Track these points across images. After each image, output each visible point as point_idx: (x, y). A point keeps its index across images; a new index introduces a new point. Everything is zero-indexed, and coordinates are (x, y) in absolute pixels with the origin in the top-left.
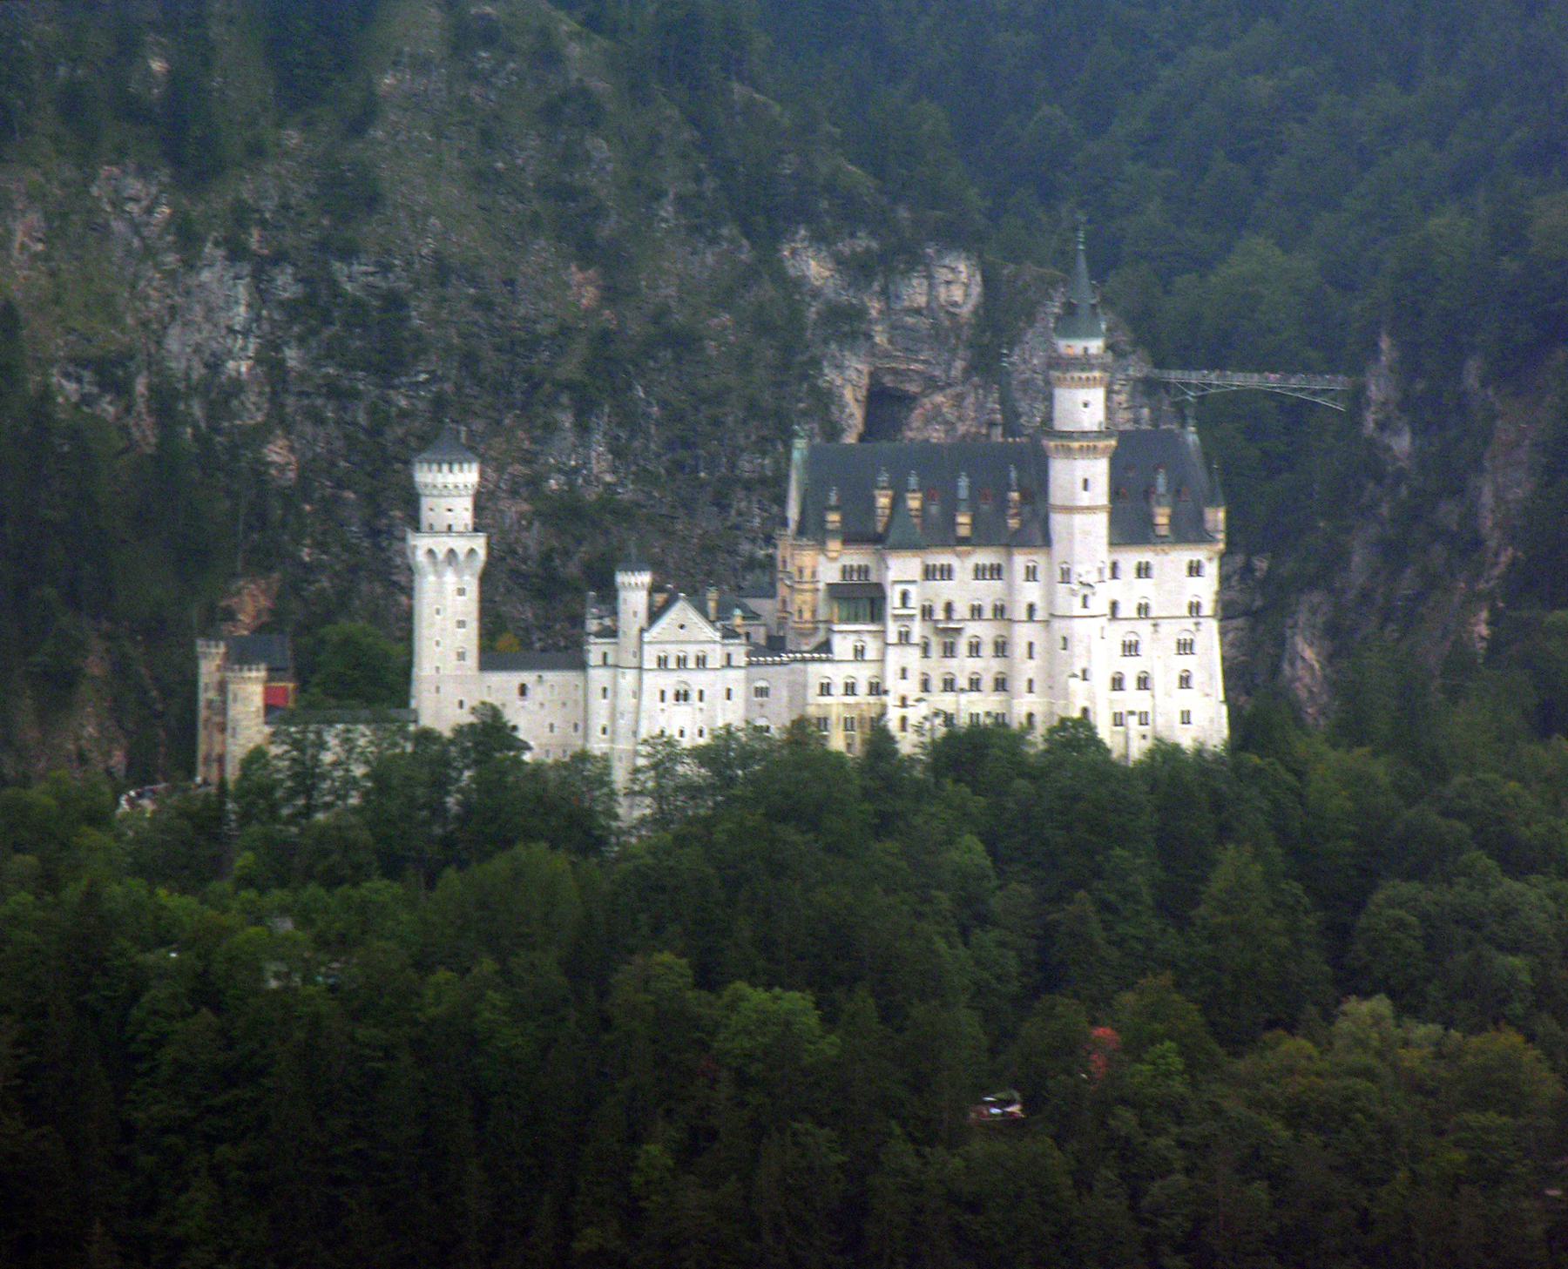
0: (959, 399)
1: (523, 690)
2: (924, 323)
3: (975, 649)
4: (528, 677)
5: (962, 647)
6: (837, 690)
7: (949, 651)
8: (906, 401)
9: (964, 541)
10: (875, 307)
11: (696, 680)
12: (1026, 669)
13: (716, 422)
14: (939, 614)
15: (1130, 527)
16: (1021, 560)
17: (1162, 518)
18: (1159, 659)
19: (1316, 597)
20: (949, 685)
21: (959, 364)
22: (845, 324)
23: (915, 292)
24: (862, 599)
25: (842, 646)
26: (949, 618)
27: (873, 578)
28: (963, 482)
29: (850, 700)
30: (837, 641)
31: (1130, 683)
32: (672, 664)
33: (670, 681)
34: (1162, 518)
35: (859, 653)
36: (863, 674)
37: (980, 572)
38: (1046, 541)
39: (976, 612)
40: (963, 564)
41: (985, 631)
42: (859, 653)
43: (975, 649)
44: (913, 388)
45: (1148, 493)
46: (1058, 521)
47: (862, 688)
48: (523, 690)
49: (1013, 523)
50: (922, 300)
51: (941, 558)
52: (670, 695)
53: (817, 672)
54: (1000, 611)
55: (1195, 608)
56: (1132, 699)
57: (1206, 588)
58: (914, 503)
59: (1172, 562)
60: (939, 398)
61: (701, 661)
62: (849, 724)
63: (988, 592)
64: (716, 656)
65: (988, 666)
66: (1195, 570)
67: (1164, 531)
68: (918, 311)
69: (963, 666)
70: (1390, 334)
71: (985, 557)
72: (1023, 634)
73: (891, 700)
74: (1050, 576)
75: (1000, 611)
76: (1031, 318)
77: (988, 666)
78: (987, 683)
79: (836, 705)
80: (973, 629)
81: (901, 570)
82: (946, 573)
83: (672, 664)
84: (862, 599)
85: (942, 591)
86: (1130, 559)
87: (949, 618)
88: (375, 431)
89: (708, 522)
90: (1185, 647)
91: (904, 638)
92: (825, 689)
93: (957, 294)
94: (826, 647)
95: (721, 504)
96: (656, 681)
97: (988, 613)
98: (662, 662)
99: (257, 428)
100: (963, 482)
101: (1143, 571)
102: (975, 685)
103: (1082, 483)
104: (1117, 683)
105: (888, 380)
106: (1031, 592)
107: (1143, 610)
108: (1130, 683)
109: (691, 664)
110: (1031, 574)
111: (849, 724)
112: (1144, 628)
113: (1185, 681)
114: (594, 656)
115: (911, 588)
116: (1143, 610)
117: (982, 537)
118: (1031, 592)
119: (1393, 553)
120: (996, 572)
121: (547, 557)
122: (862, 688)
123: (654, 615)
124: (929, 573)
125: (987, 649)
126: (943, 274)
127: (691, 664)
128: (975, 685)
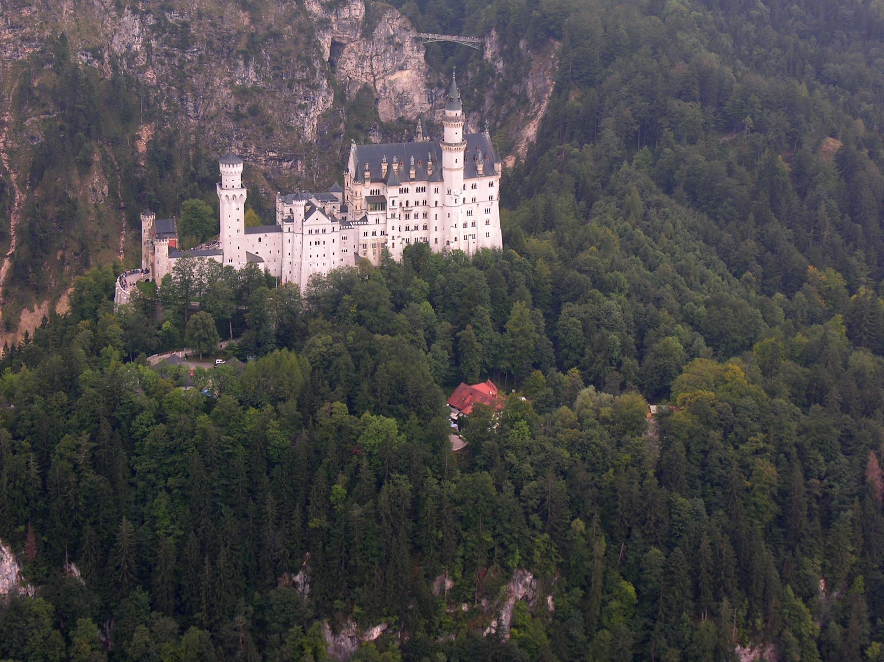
0: (359, 44)
1: (260, 240)
2: (349, 22)
3: (416, 216)
4: (262, 235)
5: (412, 216)
6: (370, 234)
7: (407, 217)
8: (342, 46)
9: (413, 180)
10: (333, 19)
11: (321, 237)
12: (434, 223)
13: (288, 61)
14: (404, 205)
15: (470, 172)
16: (433, 186)
17: (480, 168)
18: (479, 216)
19: (475, 114)
20: (407, 229)
21: (359, 34)
22: (324, 24)
23: (345, 13)
24: (378, 202)
25: (371, 219)
26: (407, 205)
27: (381, 194)
28: (412, 159)
29: (374, 237)
30: (369, 218)
31: (469, 225)
32: (314, 232)
33: (314, 238)
34: (480, 168)
35: (377, 221)
36: (379, 229)
37: (418, 190)
38: (442, 180)
39: (417, 203)
40: (412, 187)
41: (420, 210)
42: (377, 221)
43: (416, 216)
44: (344, 42)
45: (475, 158)
46: (445, 173)
47: (378, 233)
48: (260, 240)
49: (430, 173)
50: (347, 16)
51: (404, 186)
52: (313, 243)
53: (363, 229)
54: (425, 203)
55: (491, 198)
56: (470, 230)
57: (495, 191)
58: (395, 167)
59: (482, 182)
60: (352, 45)
61: (324, 231)
62: (374, 246)
63: (421, 197)
64: (329, 229)
65: (421, 222)
66: (491, 185)
67: (481, 173)
68: (346, 19)
69: (412, 222)
70: (496, 30)
71: (420, 184)
72: (433, 211)
73: (389, 238)
74: (443, 191)
75: (425, 203)
76: (380, 20)
77: (421, 222)
78: (421, 227)
79: (370, 239)
80: (416, 209)
81: (391, 193)
82: (407, 191)
83: (314, 232)
84: (378, 202)
85: (405, 197)
86: (470, 183)
87: (407, 205)
88: (181, 67)
89: (286, 93)
90: (487, 211)
91: (393, 216)
92: (366, 234)
93: (358, 13)
94: (365, 219)
95: (290, 87)
96: (308, 238)
97: (421, 203)
98: (310, 232)
99: (143, 66)
100: (412, 159)
101: (474, 187)
102: (416, 228)
103: (454, 160)
104: (465, 225)
105: (337, 40)
106: (437, 197)
107: (474, 200)
108: (469, 225)
109: (320, 232)
110: (436, 191)
111: (374, 246)
112: (475, 205)
113: (487, 223)
114: (285, 229)
115: (395, 199)
116: (474, 200)
117: (419, 177)
118: (437, 197)
119: (499, 100)
120: (424, 189)
121: (237, 108)
122: (378, 233)
123: (308, 214)
124: (401, 191)
125: (421, 216)
126: (354, 7)
127: (320, 232)
128: (416, 228)
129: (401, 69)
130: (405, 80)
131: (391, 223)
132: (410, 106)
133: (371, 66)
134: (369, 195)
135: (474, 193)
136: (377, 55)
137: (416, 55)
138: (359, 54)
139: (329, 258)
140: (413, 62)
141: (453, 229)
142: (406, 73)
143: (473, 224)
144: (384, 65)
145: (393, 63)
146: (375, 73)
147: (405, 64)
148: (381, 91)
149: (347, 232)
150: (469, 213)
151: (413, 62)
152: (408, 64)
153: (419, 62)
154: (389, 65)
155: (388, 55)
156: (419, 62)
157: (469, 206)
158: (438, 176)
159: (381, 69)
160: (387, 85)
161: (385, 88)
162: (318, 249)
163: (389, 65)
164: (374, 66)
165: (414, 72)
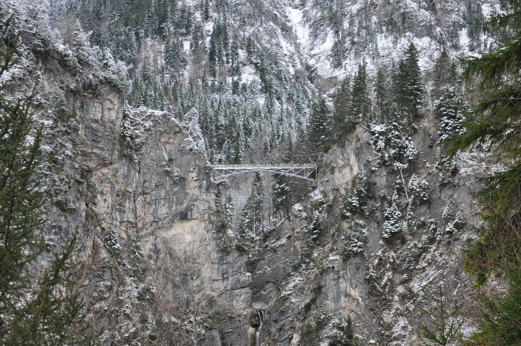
50: (99, 116)
60: (105, 171)
68: (96, 121)
126: (108, 104)
129: (184, 217)
130: (188, 238)
132: (197, 282)
133: (134, 211)
136: (144, 193)
137: (204, 196)
138: (117, 188)
140: (202, 207)
142: (187, 225)
144: (156, 210)
145: (170, 208)
146: (140, 225)
147: (189, 209)
148: (150, 257)
151: (202, 206)
152: (195, 209)
153: (210, 208)
154: (163, 211)
155: (163, 193)
156: (210, 208)
159: (149, 219)
160: (160, 246)
161: (157, 251)
163: (163, 211)
164: (139, 214)
165: (203, 225)
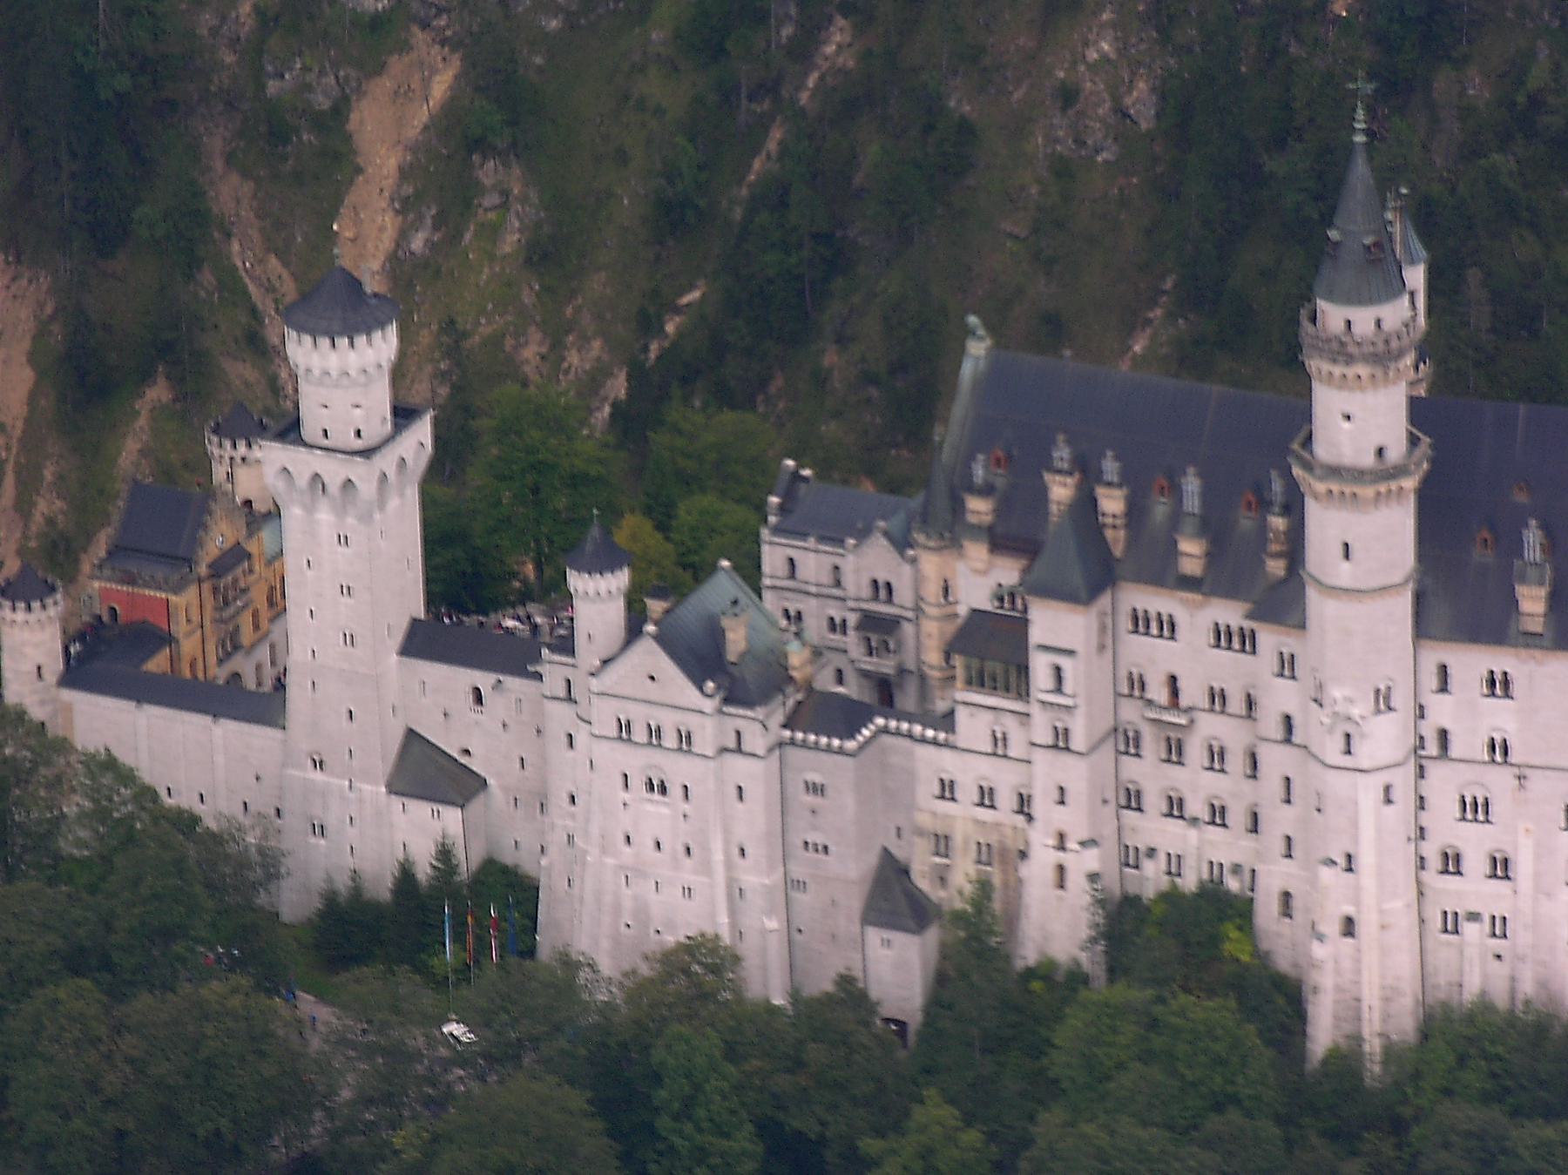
4: (484, 680)
5: (1195, 752)
11: (677, 769)
16: (1270, 639)
20: (1175, 807)
28: (1192, 485)
29: (984, 814)
30: (962, 715)
33: (637, 761)
35: (999, 743)
36: (1006, 780)
37: (1222, 637)
42: (999, 743)
46: (1314, 599)
52: (637, 782)
53: (931, 762)
67: (1536, 626)
71: (1230, 614)
79: (962, 815)
80: (1210, 727)
82: (1168, 628)
100: (1192, 485)
101: (1498, 685)
106: (1281, 697)
128: (1218, 815)
131: (1047, 771)
134: (987, 605)
135: (1501, 717)
139: (706, 868)
141: (1326, 873)
143: (1501, 867)
149: (824, 761)
150: (1475, 809)
157: (1467, 772)
158: (1282, 602)
162: (656, 816)
